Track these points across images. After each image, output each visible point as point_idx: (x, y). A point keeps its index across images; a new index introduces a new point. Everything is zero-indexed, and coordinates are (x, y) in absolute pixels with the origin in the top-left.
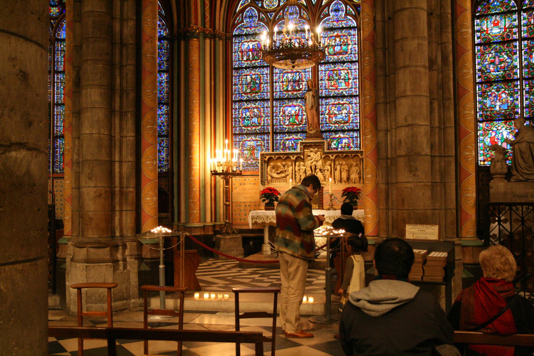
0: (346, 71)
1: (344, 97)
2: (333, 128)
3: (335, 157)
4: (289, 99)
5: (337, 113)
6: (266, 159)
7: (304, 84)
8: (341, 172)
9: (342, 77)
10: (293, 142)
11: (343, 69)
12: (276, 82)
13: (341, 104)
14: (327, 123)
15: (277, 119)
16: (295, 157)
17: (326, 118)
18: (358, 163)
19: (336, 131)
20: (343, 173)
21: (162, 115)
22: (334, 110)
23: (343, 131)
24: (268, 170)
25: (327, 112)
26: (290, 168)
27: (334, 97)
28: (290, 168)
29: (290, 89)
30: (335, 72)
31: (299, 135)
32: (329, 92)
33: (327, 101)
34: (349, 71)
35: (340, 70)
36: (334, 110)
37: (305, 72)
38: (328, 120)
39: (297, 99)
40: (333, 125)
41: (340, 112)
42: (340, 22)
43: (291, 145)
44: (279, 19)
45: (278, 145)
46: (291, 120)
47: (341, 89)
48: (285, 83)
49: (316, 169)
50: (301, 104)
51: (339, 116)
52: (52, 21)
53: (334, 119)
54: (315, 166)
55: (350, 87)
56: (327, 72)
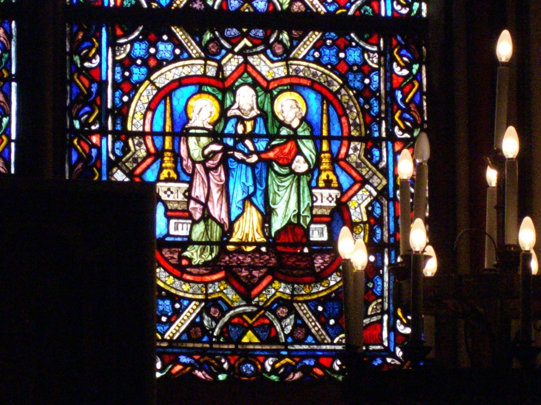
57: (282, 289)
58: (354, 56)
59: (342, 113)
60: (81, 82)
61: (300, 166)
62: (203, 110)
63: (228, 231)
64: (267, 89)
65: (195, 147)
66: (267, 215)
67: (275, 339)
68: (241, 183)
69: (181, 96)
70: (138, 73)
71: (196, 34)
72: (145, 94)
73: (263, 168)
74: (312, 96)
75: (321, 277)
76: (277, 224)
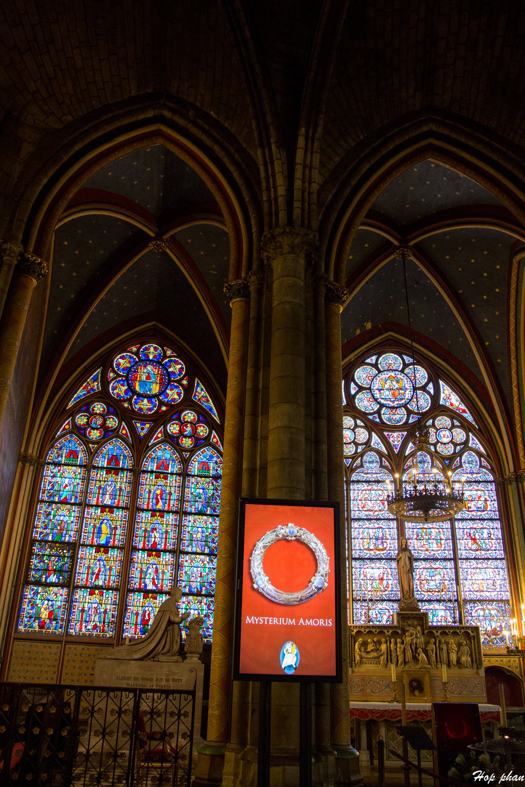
0: (437, 531)
1: (436, 559)
2: (426, 597)
3: (441, 633)
4: (371, 559)
5: (430, 578)
6: (354, 633)
7: (388, 543)
8: (448, 653)
9: (433, 537)
10: (377, 613)
11: (433, 528)
12: (354, 539)
13: (433, 568)
14: (418, 591)
15: (357, 583)
16: (391, 631)
17: (417, 585)
18: (468, 641)
19: (429, 601)
20: (451, 654)
21: (214, 569)
22: (425, 574)
23: (439, 601)
24: (356, 647)
25: (418, 577)
26: (383, 647)
27: (425, 560)
28: (383, 647)
29: (372, 547)
30: (425, 530)
31: (384, 603)
32: (418, 553)
33: (417, 564)
34: (441, 530)
35: (430, 528)
36: (425, 574)
37: (389, 528)
38: (418, 587)
39: (380, 559)
40: (426, 594)
41: (433, 578)
42: (427, 475)
43: (375, 616)
44: (357, 467)
45: (359, 615)
46: (374, 584)
47: (433, 550)
48: (365, 540)
49: (416, 648)
50: (386, 567)
51: (432, 583)
52: (90, 445)
53: (426, 587)
54: (416, 643)
55: (442, 548)
56: (415, 530)
57: (494, 637)
58: (500, 605)
59: (500, 612)
60: (466, 610)
61: (495, 620)
62: (481, 613)
63: (486, 629)
64: (489, 610)
65: (481, 618)
66: (491, 627)
67: (493, 643)
68: (487, 622)
69: (479, 611)
70: (473, 608)
71: (480, 603)
72: (474, 611)
73: (490, 620)
74: (496, 611)
75: (499, 635)
76: (493, 628)
